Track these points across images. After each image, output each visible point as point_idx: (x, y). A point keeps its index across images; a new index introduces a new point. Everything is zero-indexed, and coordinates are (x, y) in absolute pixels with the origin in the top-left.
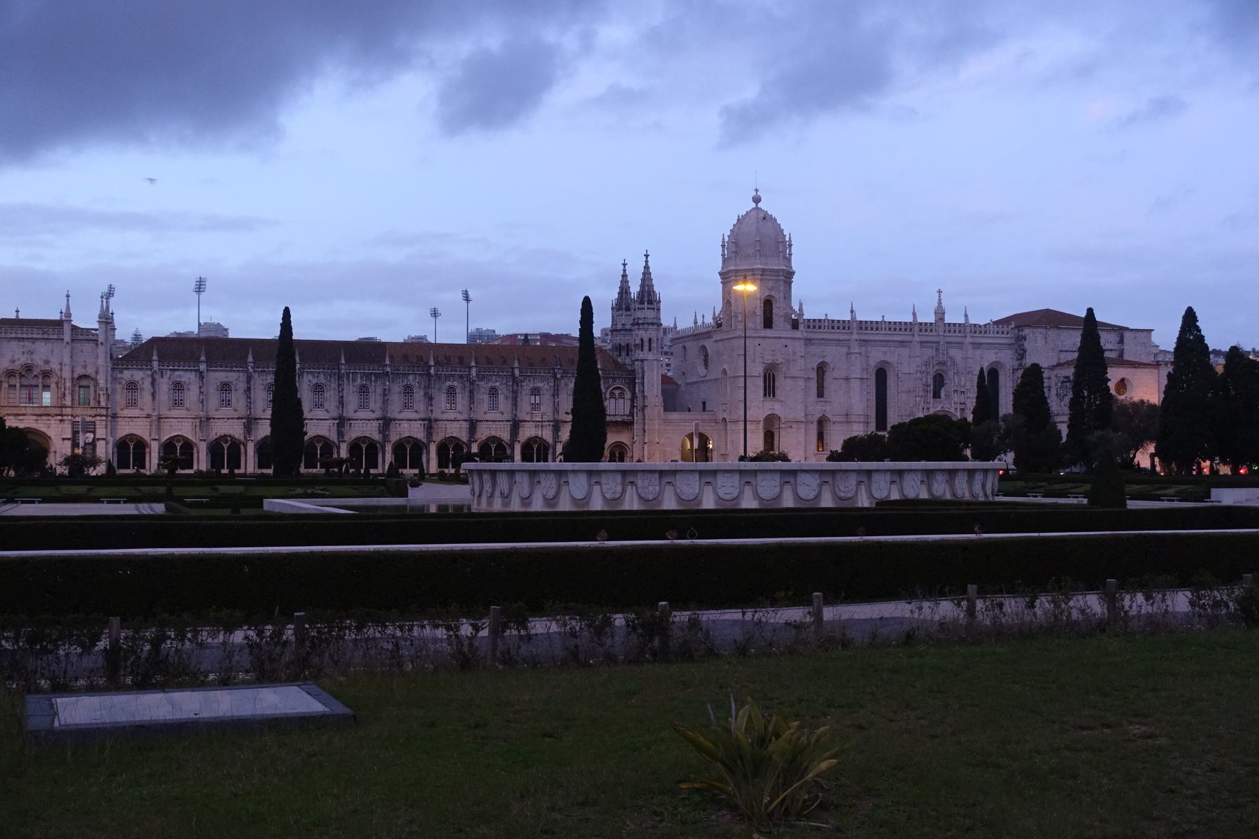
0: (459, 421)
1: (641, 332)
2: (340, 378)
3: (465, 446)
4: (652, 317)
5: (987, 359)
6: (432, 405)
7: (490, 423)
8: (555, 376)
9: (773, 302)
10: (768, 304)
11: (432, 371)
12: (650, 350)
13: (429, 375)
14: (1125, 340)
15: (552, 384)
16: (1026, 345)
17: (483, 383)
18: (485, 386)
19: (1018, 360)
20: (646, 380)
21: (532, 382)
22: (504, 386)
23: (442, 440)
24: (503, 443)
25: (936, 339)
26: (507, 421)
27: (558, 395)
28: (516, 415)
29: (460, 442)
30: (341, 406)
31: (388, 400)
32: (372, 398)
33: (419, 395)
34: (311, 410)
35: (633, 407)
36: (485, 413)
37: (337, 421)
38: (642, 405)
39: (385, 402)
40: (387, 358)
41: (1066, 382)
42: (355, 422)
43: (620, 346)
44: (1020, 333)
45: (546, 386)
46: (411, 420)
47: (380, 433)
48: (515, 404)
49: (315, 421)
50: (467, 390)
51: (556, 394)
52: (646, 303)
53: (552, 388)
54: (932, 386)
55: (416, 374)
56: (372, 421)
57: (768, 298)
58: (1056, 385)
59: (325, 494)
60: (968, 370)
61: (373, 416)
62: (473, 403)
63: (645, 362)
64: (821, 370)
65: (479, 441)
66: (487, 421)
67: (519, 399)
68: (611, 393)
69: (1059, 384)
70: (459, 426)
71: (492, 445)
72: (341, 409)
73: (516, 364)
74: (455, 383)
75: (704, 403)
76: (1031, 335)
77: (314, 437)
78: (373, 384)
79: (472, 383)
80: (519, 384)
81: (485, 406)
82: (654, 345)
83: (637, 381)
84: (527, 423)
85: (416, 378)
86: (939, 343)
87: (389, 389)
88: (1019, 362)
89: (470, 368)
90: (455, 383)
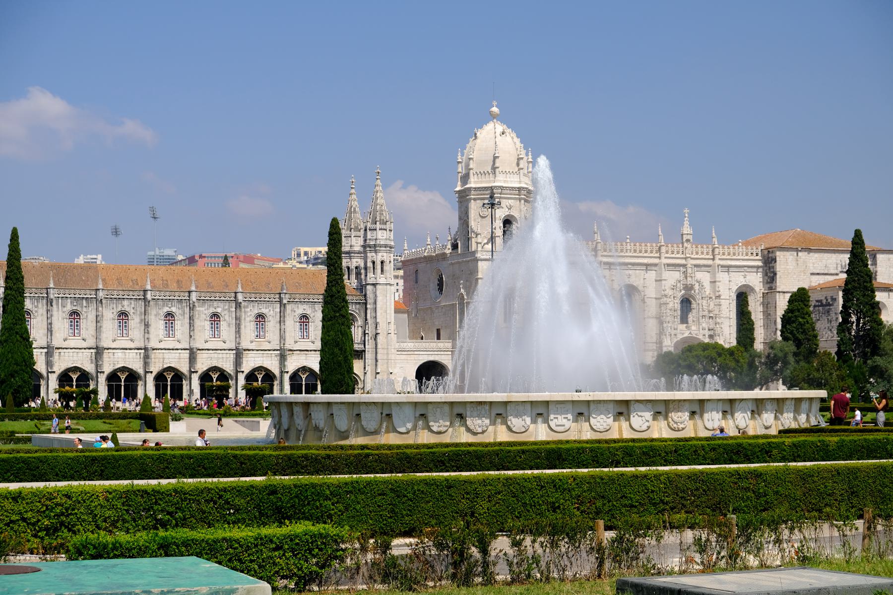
0: (177, 349)
2: (50, 302)
4: (384, 238)
5: (738, 280)
6: (148, 333)
7: (211, 352)
8: (281, 301)
9: (514, 223)
11: (149, 296)
13: (145, 299)
14: (878, 262)
15: (279, 310)
16: (780, 267)
17: (203, 309)
18: (206, 312)
19: (768, 283)
20: (378, 306)
21: (256, 307)
22: (226, 312)
24: (225, 373)
25: (683, 262)
26: (229, 350)
27: (284, 322)
28: (239, 343)
29: (179, 373)
30: (49, 334)
31: (101, 327)
32: (83, 324)
33: (134, 322)
35: (365, 334)
37: (46, 350)
38: (375, 334)
39: (98, 329)
40: (100, 281)
41: (818, 306)
42: (65, 350)
44: (770, 255)
45: (272, 312)
46: (126, 349)
47: (92, 363)
48: (238, 331)
50: (187, 316)
51: (282, 321)
53: (279, 314)
54: (679, 312)
55: (131, 299)
56: (83, 350)
57: (508, 218)
59: (79, 429)
60: (717, 294)
61: (85, 345)
62: (193, 330)
63: (378, 286)
65: (200, 372)
66: (208, 350)
67: (242, 327)
71: (213, 376)
72: (49, 337)
73: (240, 289)
75: (438, 331)
76: (781, 257)
78: (85, 309)
79: (192, 308)
80: (243, 310)
81: (208, 333)
82: (385, 268)
83: (368, 306)
84: (251, 352)
85: (131, 303)
86: (684, 266)
87: (102, 315)
88: (768, 286)
89: (190, 292)
90: (174, 309)
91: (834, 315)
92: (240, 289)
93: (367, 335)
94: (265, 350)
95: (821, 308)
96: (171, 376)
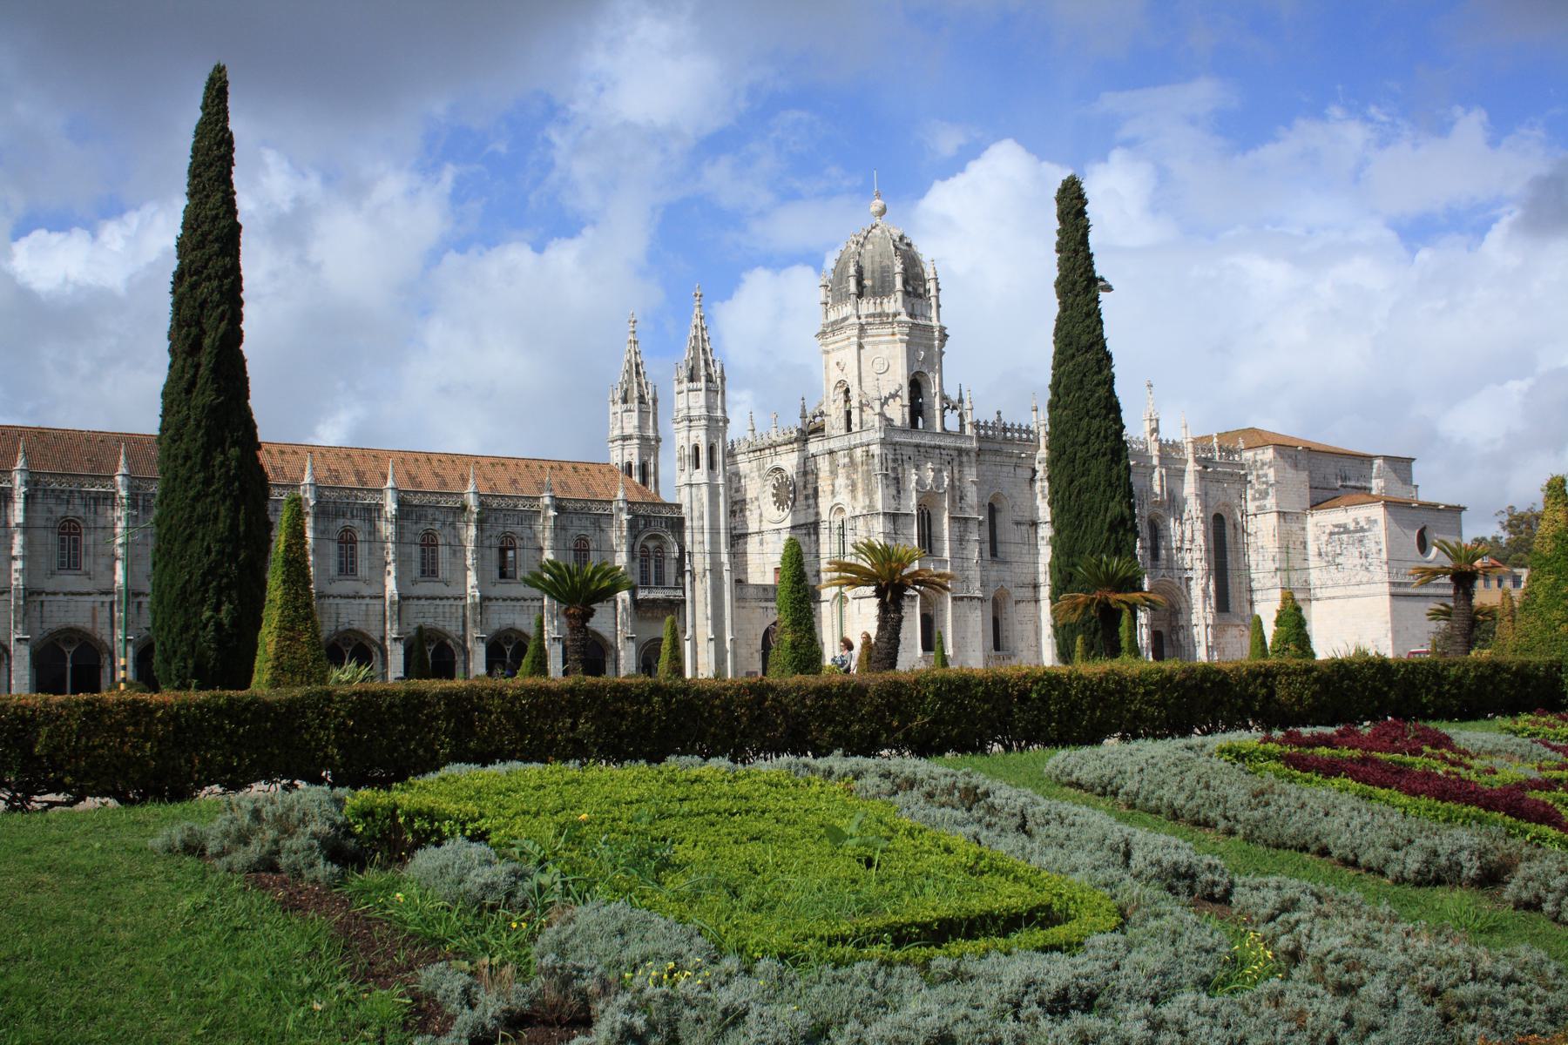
1: (693, 433)
3: (375, 649)
7: (423, 602)
9: (923, 384)
10: (916, 386)
12: (712, 465)
19: (1254, 499)
23: (331, 636)
24: (449, 641)
29: (366, 643)
34: (53, 573)
36: (414, 582)
41: (1339, 533)
43: (630, 465)
49: (61, 597)
52: (703, 379)
58: (1318, 539)
64: (992, 511)
66: (419, 598)
68: (643, 546)
69: (1324, 538)
70: (364, 608)
74: (357, 522)
77: (60, 632)
83: (688, 523)
84: (494, 602)
88: (1257, 503)
91: (1373, 545)
92: (471, 488)
93: (688, 575)
94: (518, 600)
95: (1344, 537)
96: (350, 649)
